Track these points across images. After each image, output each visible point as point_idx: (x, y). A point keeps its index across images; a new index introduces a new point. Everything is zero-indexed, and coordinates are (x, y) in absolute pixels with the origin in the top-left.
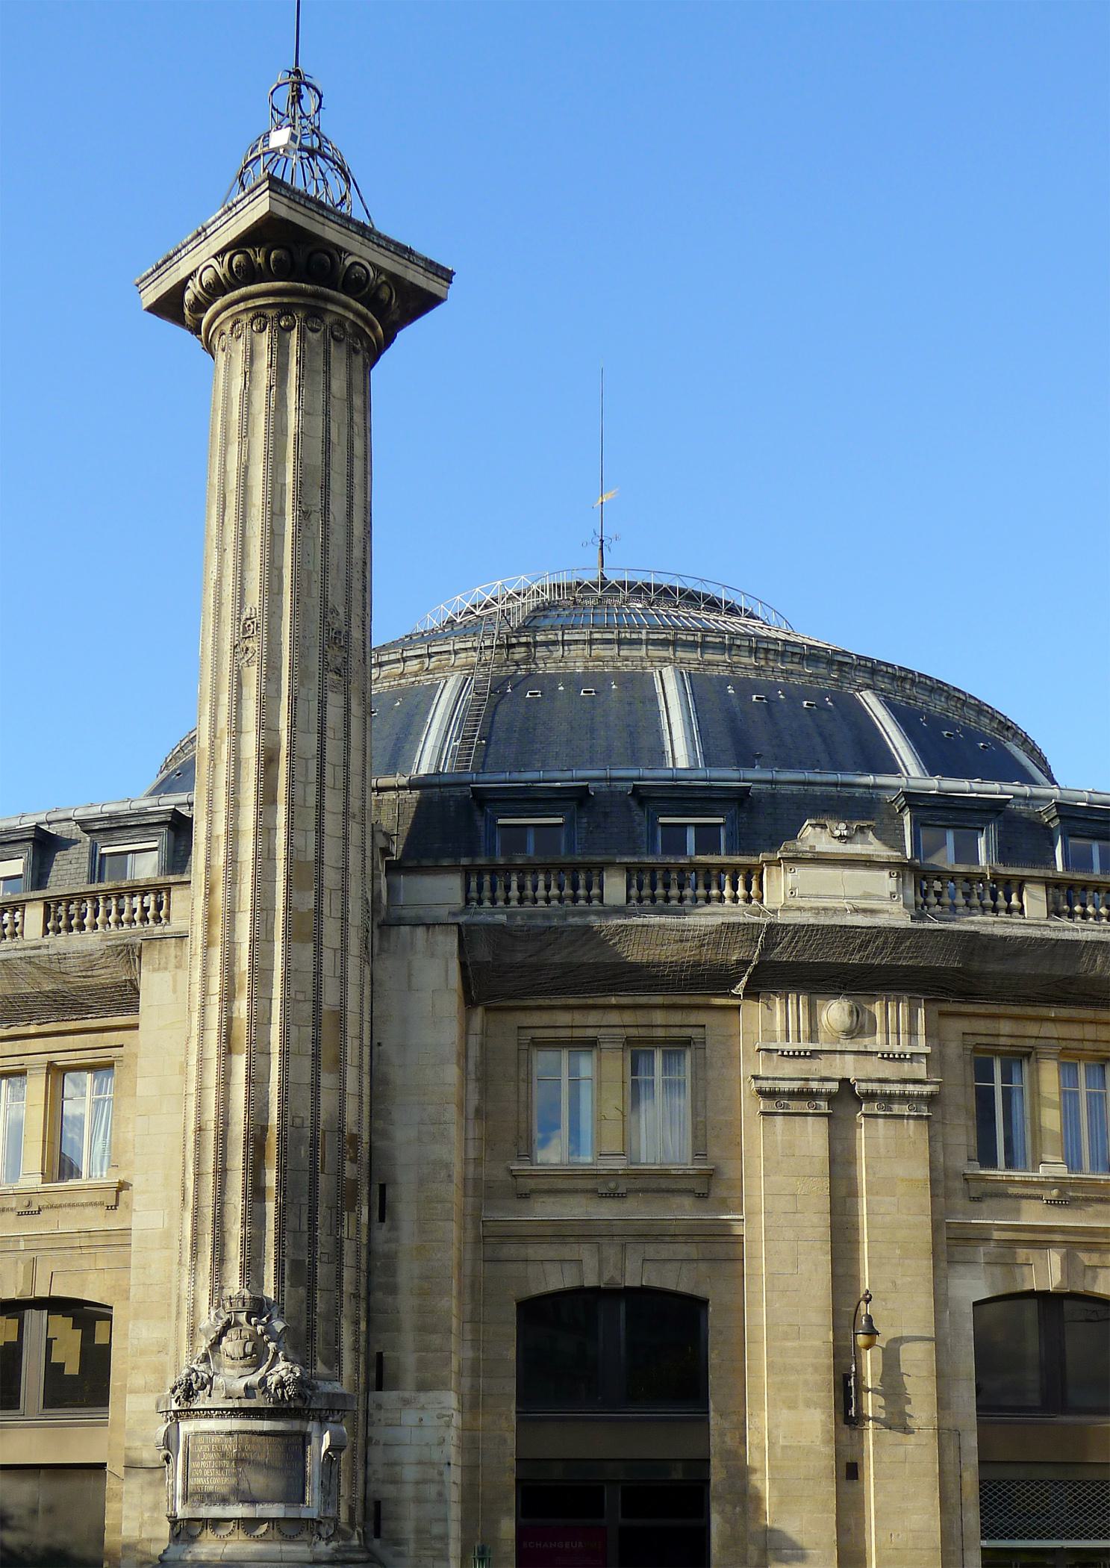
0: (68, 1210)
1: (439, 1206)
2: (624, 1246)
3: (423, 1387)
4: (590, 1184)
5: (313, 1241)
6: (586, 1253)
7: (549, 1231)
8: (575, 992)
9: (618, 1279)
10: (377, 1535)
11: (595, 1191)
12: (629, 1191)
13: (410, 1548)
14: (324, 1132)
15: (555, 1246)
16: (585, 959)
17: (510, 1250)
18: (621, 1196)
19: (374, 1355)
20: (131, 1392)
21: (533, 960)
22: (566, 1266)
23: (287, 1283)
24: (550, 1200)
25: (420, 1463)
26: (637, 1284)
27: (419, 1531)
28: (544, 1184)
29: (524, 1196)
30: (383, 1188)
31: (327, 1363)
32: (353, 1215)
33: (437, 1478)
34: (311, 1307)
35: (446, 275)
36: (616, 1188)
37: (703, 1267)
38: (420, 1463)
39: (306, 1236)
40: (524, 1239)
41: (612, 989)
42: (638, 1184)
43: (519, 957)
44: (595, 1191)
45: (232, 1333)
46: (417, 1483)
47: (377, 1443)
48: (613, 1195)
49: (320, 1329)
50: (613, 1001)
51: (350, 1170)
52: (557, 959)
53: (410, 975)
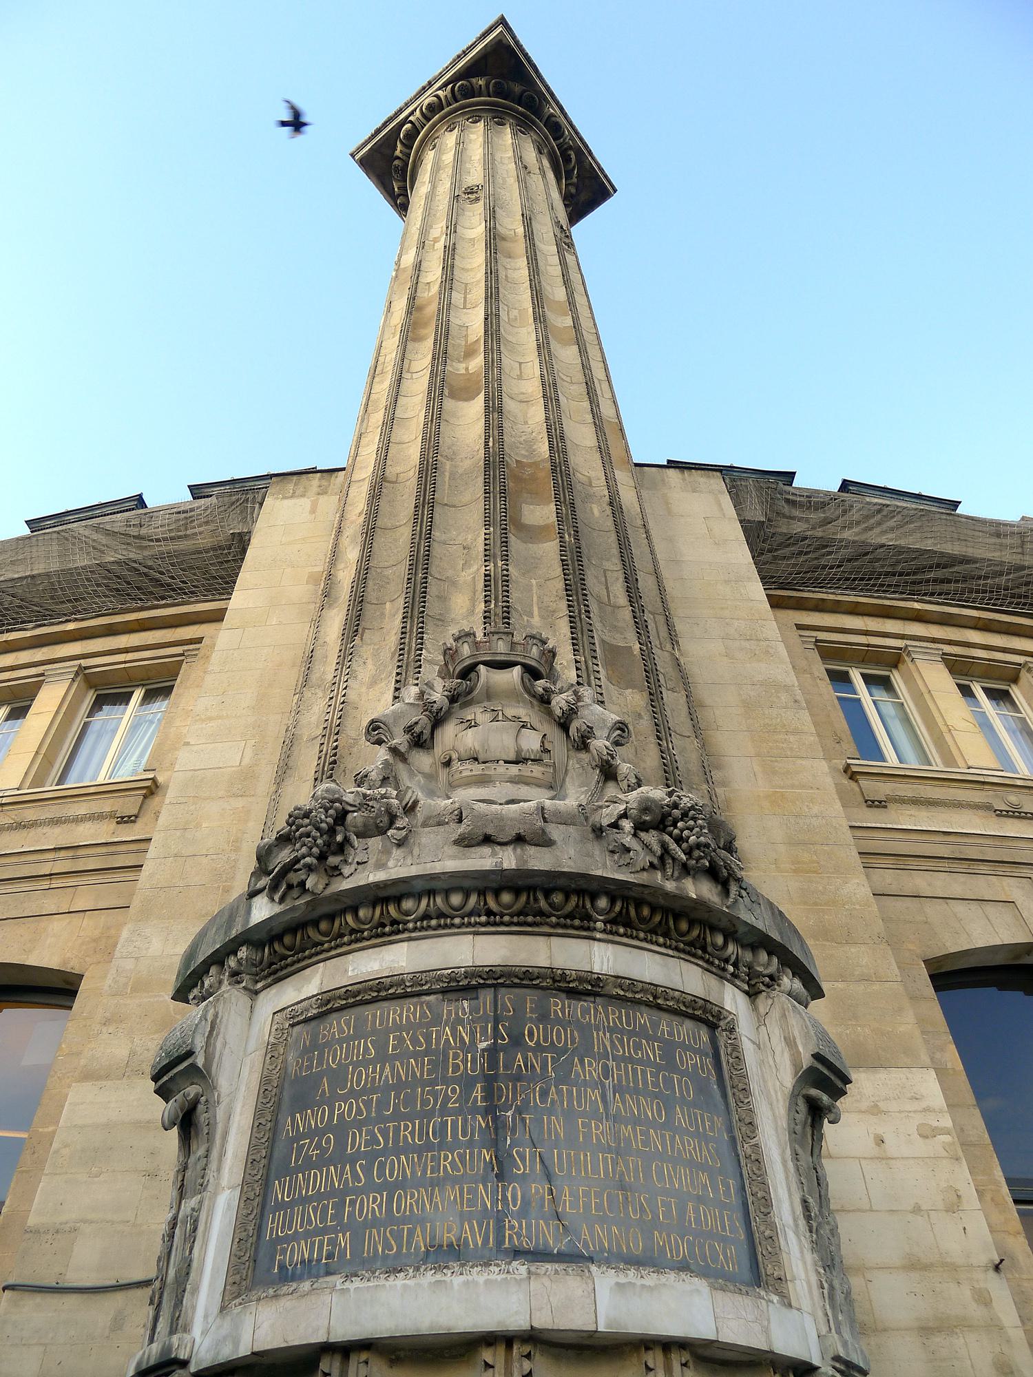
0: (46, 829)
1: (792, 738)
8: (866, 590)
15: (962, 878)
20: (88, 1076)
21: (819, 533)
22: (990, 909)
25: (914, 1265)
33: (976, 1312)
38: (914, 1265)
39: (627, 614)
41: (913, 592)
43: (798, 528)
44: (988, 807)
45: (475, 713)
46: (926, 1330)
52: (847, 535)
53: (667, 503)
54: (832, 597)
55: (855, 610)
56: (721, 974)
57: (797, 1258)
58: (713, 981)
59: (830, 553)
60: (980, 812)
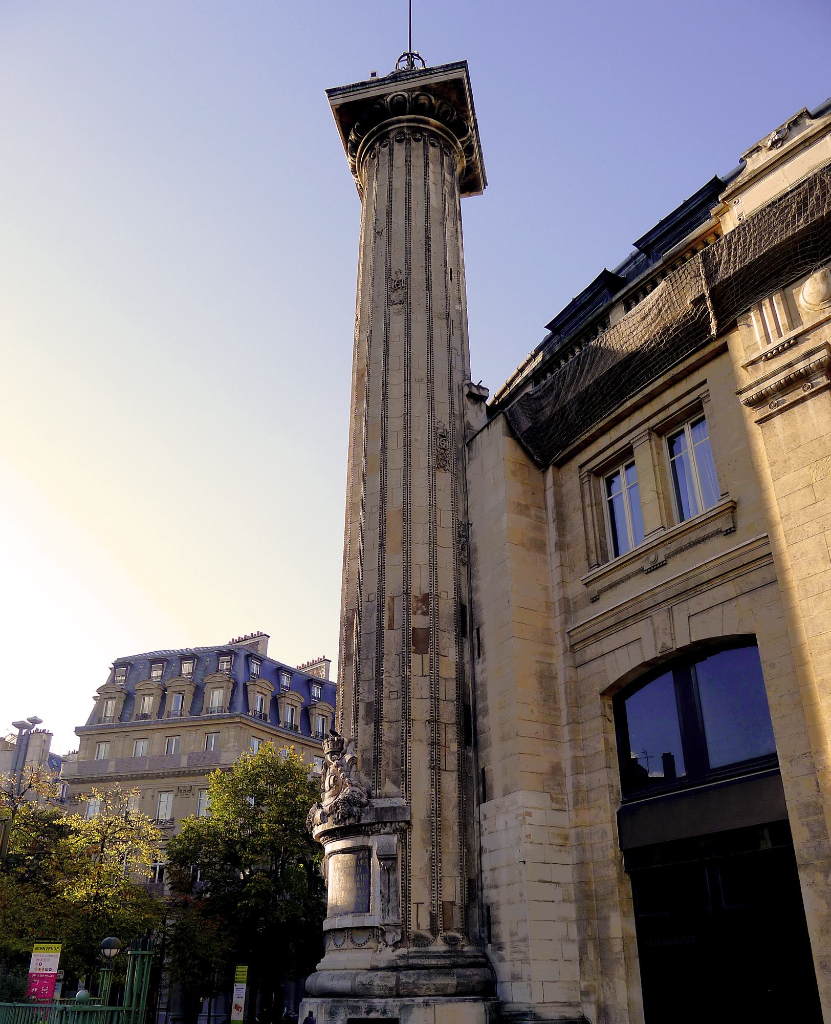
2: (670, 611)
3: (506, 792)
4: (636, 566)
5: (379, 683)
6: (641, 629)
7: (611, 621)
9: (669, 644)
10: (490, 942)
11: (641, 570)
12: (668, 557)
13: (506, 953)
14: (393, 598)
16: (587, 383)
17: (592, 651)
18: (663, 564)
19: (480, 771)
21: (558, 407)
22: (631, 647)
23: (361, 722)
24: (610, 594)
26: (687, 642)
27: (512, 934)
28: (605, 582)
29: (595, 600)
30: (478, 630)
31: (395, 782)
32: (427, 657)
34: (377, 736)
35: (463, 65)
36: (656, 560)
37: (743, 600)
40: (596, 636)
41: (622, 395)
42: (674, 547)
43: (548, 411)
47: (485, 852)
48: (656, 566)
49: (389, 754)
50: (628, 404)
51: (419, 621)
52: (570, 396)
54: (588, 435)
55: (603, 431)
56: (369, 836)
57: (376, 903)
58: (366, 838)
59: (569, 415)
60: (639, 576)
